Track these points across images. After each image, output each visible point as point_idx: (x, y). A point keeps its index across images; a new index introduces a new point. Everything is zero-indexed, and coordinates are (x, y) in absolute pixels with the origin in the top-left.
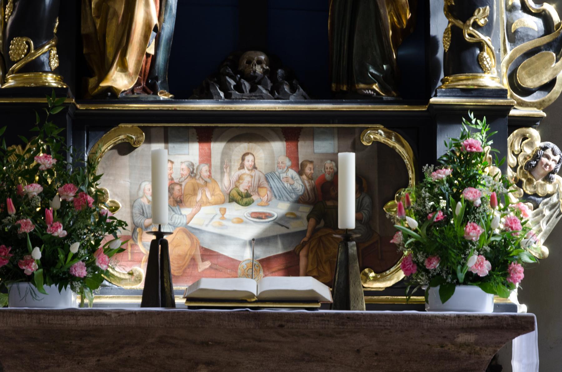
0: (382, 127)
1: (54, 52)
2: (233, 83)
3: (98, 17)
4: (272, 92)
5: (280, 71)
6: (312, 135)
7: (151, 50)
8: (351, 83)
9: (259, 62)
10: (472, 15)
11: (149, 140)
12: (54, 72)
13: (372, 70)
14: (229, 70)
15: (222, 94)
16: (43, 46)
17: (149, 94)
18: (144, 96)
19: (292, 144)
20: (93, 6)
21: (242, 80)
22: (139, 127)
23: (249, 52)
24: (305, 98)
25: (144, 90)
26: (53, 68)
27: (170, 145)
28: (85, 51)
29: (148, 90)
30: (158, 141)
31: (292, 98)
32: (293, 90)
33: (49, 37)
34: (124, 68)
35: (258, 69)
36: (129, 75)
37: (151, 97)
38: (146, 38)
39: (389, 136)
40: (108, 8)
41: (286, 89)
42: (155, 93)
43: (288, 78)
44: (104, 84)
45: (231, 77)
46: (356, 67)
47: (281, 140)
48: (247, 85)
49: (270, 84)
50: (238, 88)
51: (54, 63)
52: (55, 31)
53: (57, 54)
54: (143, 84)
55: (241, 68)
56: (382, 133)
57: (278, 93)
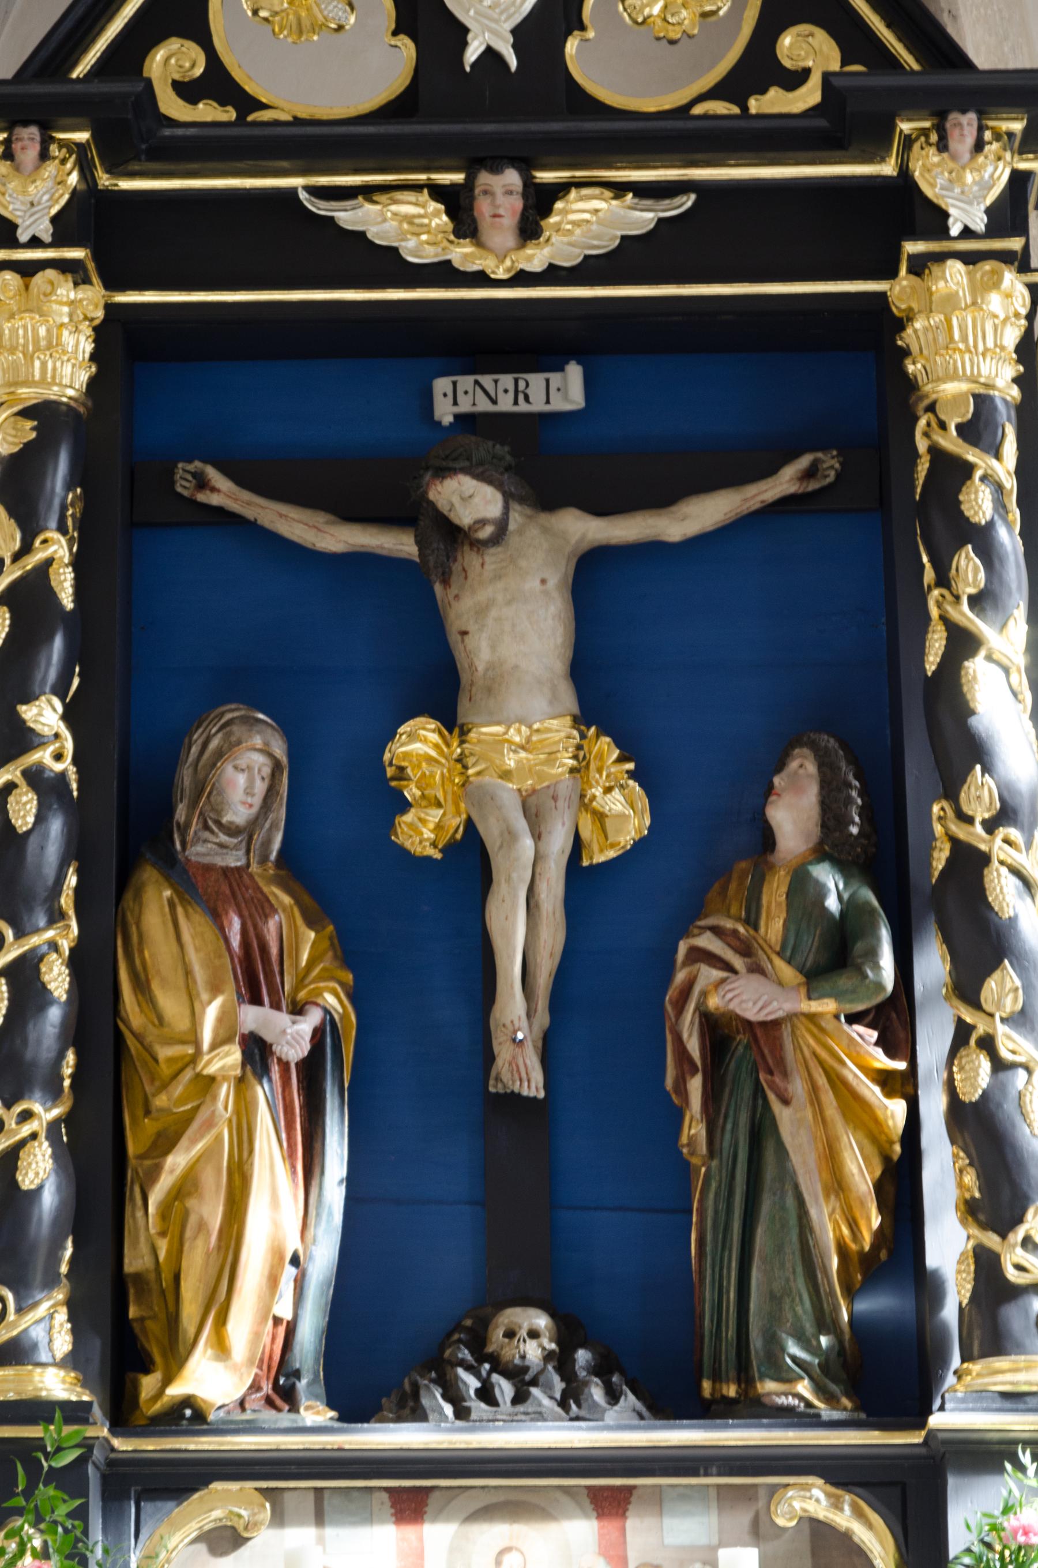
0: (820, 1482)
1: (62, 1315)
2: (472, 1383)
3: (163, 1234)
4: (563, 1404)
5: (582, 1356)
6: (657, 1501)
7: (284, 1309)
8: (745, 1377)
9: (534, 1334)
10: (1020, 1220)
11: (279, 1519)
12: (61, 1364)
13: (794, 1349)
14: (465, 1354)
15: (448, 1409)
16: (35, 1305)
17: (279, 1410)
18: (268, 1415)
19: (611, 1526)
20: (151, 1209)
21: (496, 1377)
22: (256, 1489)
23: (509, 1311)
24: (641, 1417)
25: (269, 1402)
26: (59, 1355)
27: (330, 1532)
28: (133, 1312)
29: (279, 1402)
30: (301, 1523)
31: (612, 1415)
32: (613, 1396)
33: (51, 1281)
34: (221, 1348)
35: (533, 1352)
36: (235, 1368)
37: (285, 1419)
38: (273, 1281)
39: (837, 1506)
40: (186, 1214)
41: (597, 1393)
42: (294, 1408)
43: (602, 1369)
44: (176, 1390)
45: (469, 1368)
46: (756, 1342)
47: (587, 1516)
48: (504, 1388)
49: (559, 1386)
50: (486, 1394)
51: (63, 1343)
52: (64, 1269)
53: (70, 1320)
54: (267, 1388)
55: (490, 1349)
56: (821, 1496)
57: (579, 1406)
